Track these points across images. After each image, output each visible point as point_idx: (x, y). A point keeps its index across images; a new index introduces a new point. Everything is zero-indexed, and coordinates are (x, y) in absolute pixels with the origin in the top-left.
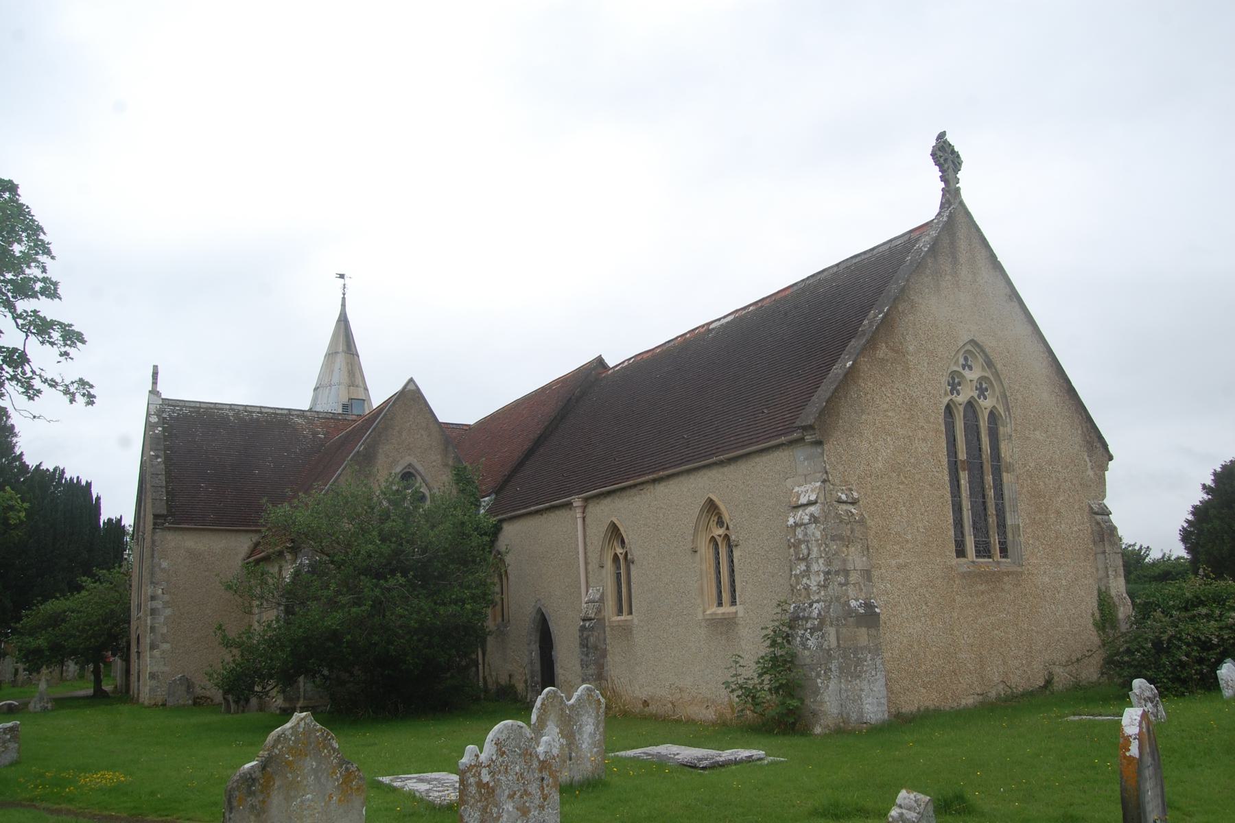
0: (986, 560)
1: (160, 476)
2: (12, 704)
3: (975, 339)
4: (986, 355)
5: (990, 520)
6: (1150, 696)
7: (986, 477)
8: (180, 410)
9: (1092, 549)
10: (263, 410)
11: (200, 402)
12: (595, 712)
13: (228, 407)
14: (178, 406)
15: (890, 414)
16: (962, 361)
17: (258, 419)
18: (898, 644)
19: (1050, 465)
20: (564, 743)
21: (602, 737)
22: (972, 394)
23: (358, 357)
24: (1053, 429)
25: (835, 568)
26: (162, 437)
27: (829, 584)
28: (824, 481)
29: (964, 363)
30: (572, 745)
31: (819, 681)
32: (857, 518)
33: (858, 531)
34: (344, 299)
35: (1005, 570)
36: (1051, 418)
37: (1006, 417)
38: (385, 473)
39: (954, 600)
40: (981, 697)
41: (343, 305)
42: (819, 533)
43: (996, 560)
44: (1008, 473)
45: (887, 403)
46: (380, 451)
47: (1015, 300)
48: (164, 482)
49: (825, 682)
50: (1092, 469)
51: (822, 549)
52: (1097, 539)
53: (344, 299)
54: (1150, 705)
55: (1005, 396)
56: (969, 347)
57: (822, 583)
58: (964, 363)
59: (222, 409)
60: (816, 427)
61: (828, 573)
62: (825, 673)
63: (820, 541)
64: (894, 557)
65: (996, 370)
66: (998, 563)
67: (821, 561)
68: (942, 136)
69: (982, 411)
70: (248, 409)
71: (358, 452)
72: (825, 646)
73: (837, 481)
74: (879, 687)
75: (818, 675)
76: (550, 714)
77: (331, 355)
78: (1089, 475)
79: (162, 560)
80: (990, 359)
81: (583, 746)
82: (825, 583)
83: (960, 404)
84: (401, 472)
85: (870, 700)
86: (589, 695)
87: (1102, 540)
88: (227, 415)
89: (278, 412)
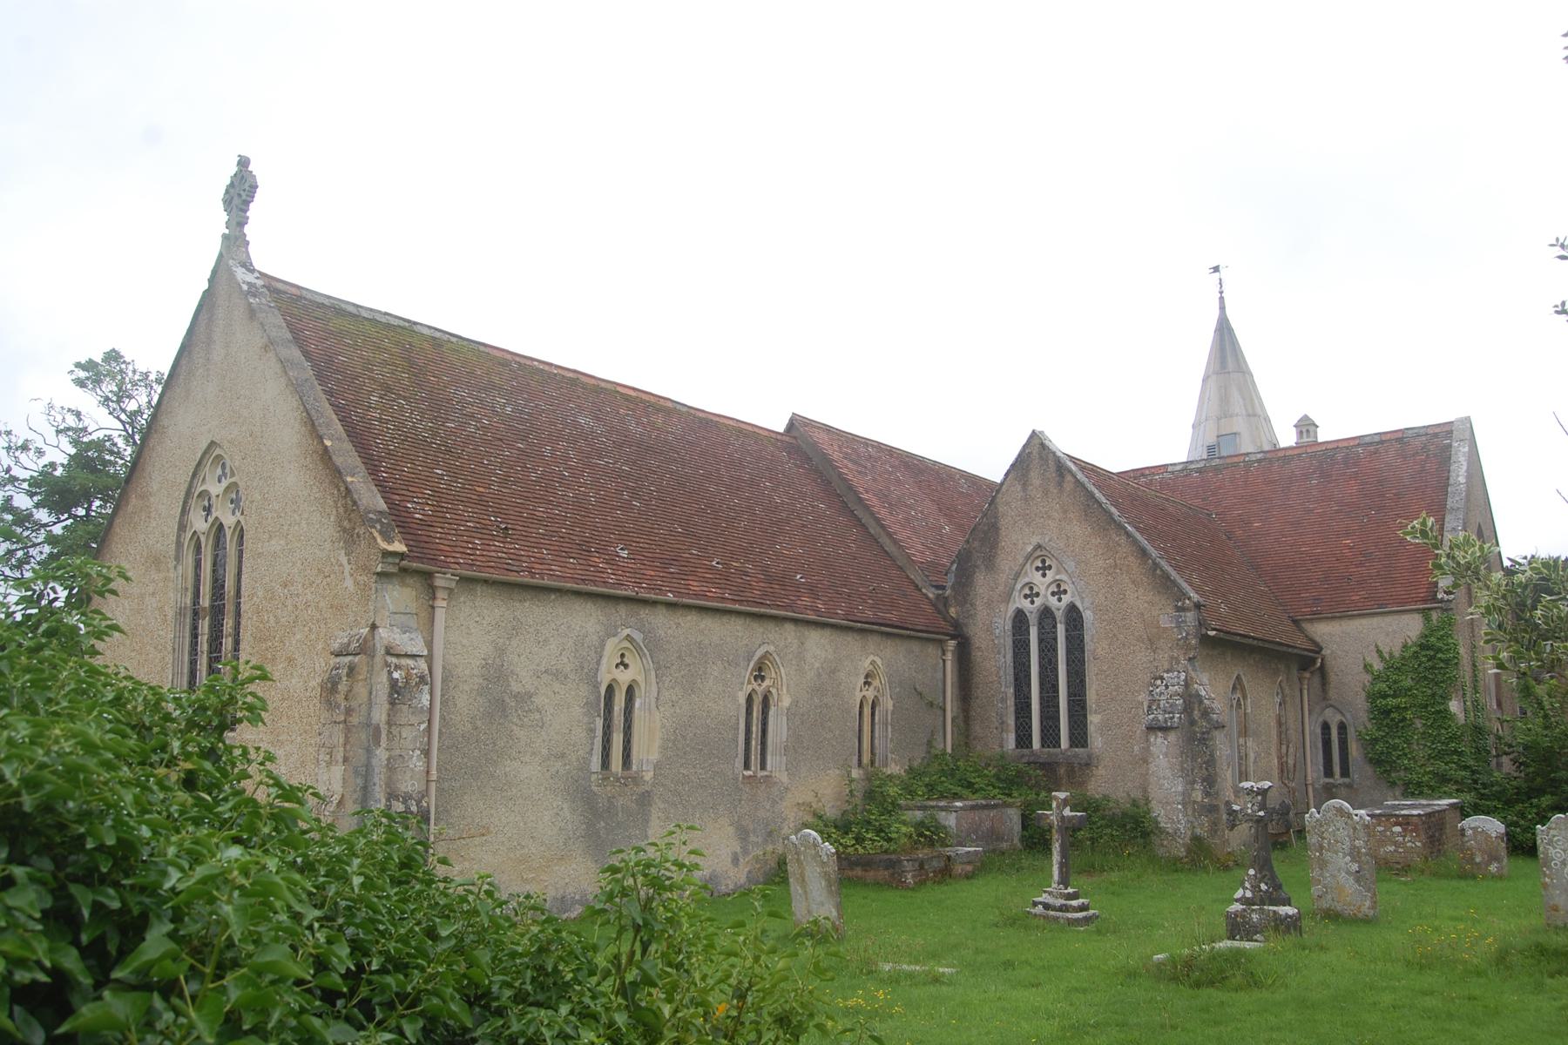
34: (1222, 299)
41: (1222, 308)
53: (1222, 299)
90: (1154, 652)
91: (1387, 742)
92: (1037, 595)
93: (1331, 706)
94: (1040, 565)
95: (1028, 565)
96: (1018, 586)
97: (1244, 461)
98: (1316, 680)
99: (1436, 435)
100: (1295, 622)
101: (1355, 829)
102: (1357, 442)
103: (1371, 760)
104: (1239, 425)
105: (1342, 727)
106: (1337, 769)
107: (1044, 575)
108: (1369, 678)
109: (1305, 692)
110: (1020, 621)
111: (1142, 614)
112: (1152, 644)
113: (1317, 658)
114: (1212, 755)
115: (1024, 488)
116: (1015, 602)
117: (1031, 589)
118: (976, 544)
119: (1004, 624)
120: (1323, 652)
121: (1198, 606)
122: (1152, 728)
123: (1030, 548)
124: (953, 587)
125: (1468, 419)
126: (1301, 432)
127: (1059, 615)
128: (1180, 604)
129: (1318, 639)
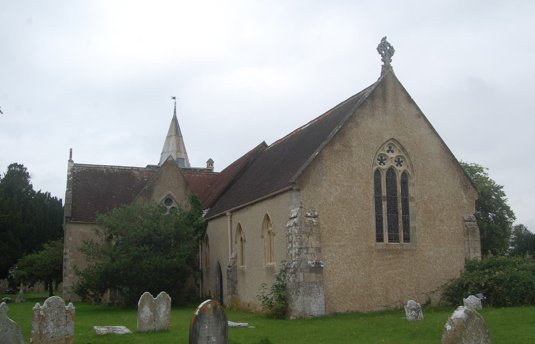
0: (396, 243)
1: (70, 200)
2: (8, 299)
3: (394, 138)
4: (401, 146)
5: (399, 225)
6: (415, 308)
7: (398, 204)
8: (82, 169)
9: (463, 239)
10: (120, 168)
11: (91, 165)
12: (166, 303)
13: (104, 167)
14: (81, 167)
15: (339, 176)
16: (388, 148)
17: (117, 172)
18: (337, 281)
19: (438, 197)
20: (152, 314)
21: (170, 313)
22: (392, 164)
23: (182, 137)
24: (442, 180)
25: (304, 246)
26: (72, 181)
27: (301, 253)
28: (301, 207)
29: (389, 149)
30: (155, 315)
31: (293, 296)
32: (315, 224)
33: (315, 230)
34: (175, 109)
35: (405, 248)
36: (440, 175)
37: (412, 174)
38: (158, 199)
39: (372, 262)
40: (386, 308)
41: (175, 112)
42: (297, 230)
43: (401, 243)
44: (412, 202)
45: (338, 171)
46: (155, 189)
47: (422, 117)
48: (71, 202)
49: (296, 297)
50: (466, 199)
51: (298, 237)
52: (466, 234)
53: (175, 109)
54: (414, 312)
55: (412, 165)
56: (391, 142)
57: (297, 253)
58: (389, 149)
59: (101, 168)
60: (296, 183)
61: (301, 248)
62: (296, 292)
63: (297, 234)
64: (337, 242)
65: (406, 152)
66: (402, 245)
67: (297, 243)
68: (384, 39)
69: (398, 172)
70: (113, 167)
71: (145, 189)
72: (297, 281)
73: (307, 207)
74: (321, 300)
75: (293, 294)
76: (146, 303)
77: (169, 137)
78: (464, 202)
79: (69, 237)
80: (403, 147)
81: (161, 316)
82: (298, 253)
83: (384, 170)
84: (165, 198)
85: (315, 306)
86: (163, 296)
87: (468, 234)
88: (103, 170)
89: (127, 168)
126: (210, 164)
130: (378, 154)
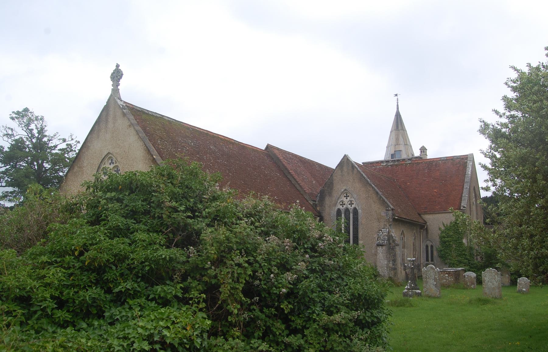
34: (398, 105)
41: (398, 108)
53: (398, 105)
90: (379, 223)
91: (445, 251)
92: (345, 204)
93: (429, 240)
94: (346, 195)
95: (342, 195)
96: (339, 202)
97: (405, 163)
98: (425, 232)
99: (463, 159)
100: (419, 214)
101: (435, 273)
102: (439, 159)
103: (440, 256)
104: (402, 148)
105: (432, 247)
106: (430, 259)
107: (347, 198)
108: (440, 232)
109: (421, 236)
110: (339, 212)
111: (376, 211)
112: (379, 220)
113: (425, 226)
114: (395, 253)
115: (342, 172)
116: (337, 206)
117: (343, 202)
118: (326, 188)
119: (334, 212)
120: (427, 224)
121: (393, 210)
122: (378, 245)
123: (343, 190)
124: (318, 201)
125: (472, 154)
126: (422, 151)
127: (351, 211)
128: (387, 209)
129: (426, 220)
130: (101, 168)
